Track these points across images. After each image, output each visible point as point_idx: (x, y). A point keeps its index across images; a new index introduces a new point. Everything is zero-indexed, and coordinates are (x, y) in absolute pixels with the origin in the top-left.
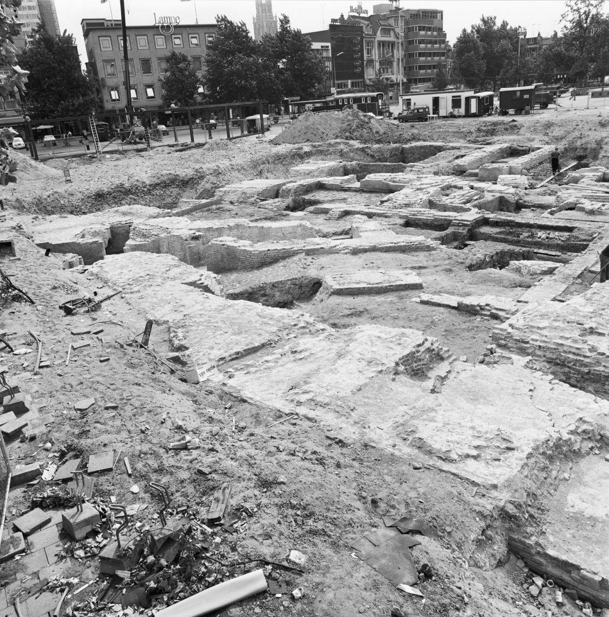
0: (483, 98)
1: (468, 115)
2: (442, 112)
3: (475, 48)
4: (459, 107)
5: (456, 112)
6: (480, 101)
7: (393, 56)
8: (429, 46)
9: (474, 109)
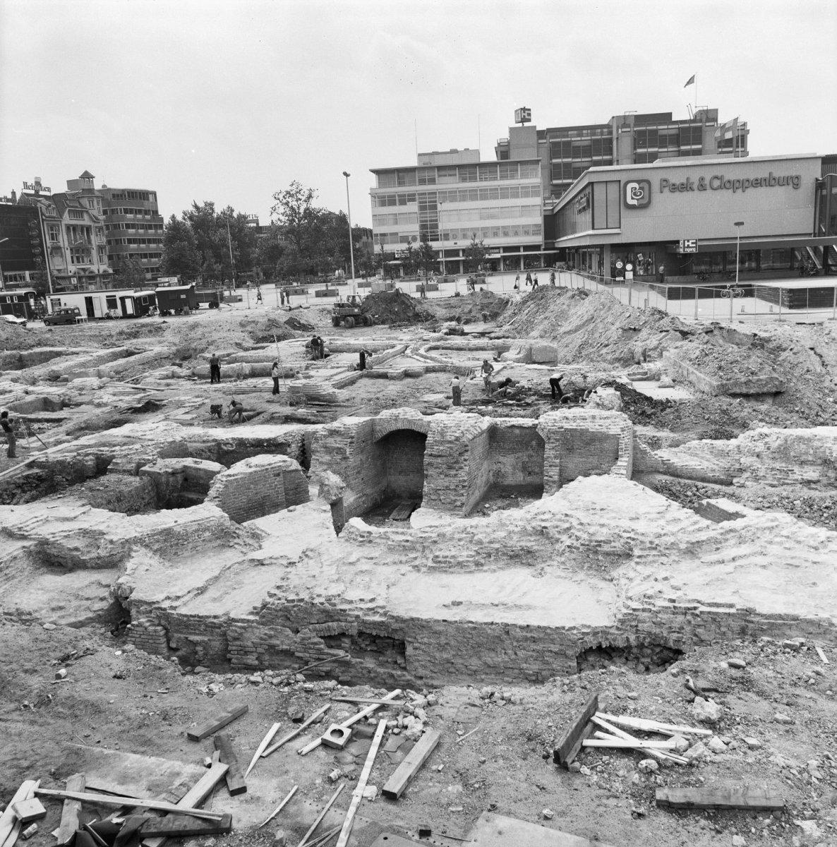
0: (139, 298)
1: (126, 316)
2: (98, 314)
3: (189, 239)
4: (116, 307)
5: (112, 313)
6: (136, 301)
7: (90, 242)
8: (141, 231)
9: (130, 310)
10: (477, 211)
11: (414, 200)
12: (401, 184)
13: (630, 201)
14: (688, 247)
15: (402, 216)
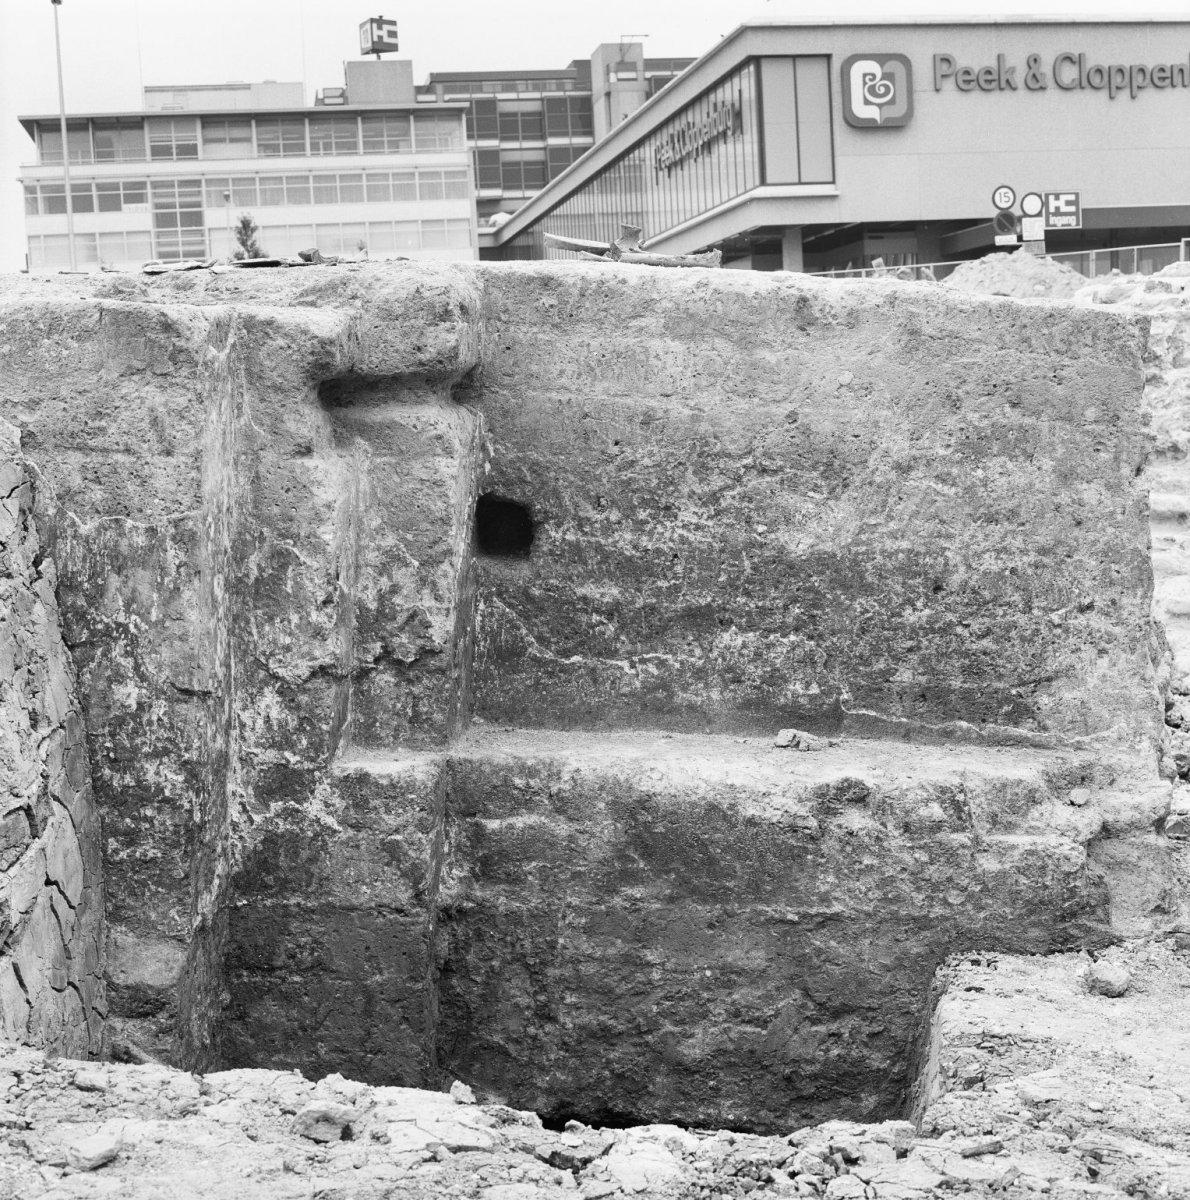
10: (306, 231)
11: (139, 198)
12: (105, 154)
13: (862, 111)
14: (1058, 213)
15: (107, 241)
